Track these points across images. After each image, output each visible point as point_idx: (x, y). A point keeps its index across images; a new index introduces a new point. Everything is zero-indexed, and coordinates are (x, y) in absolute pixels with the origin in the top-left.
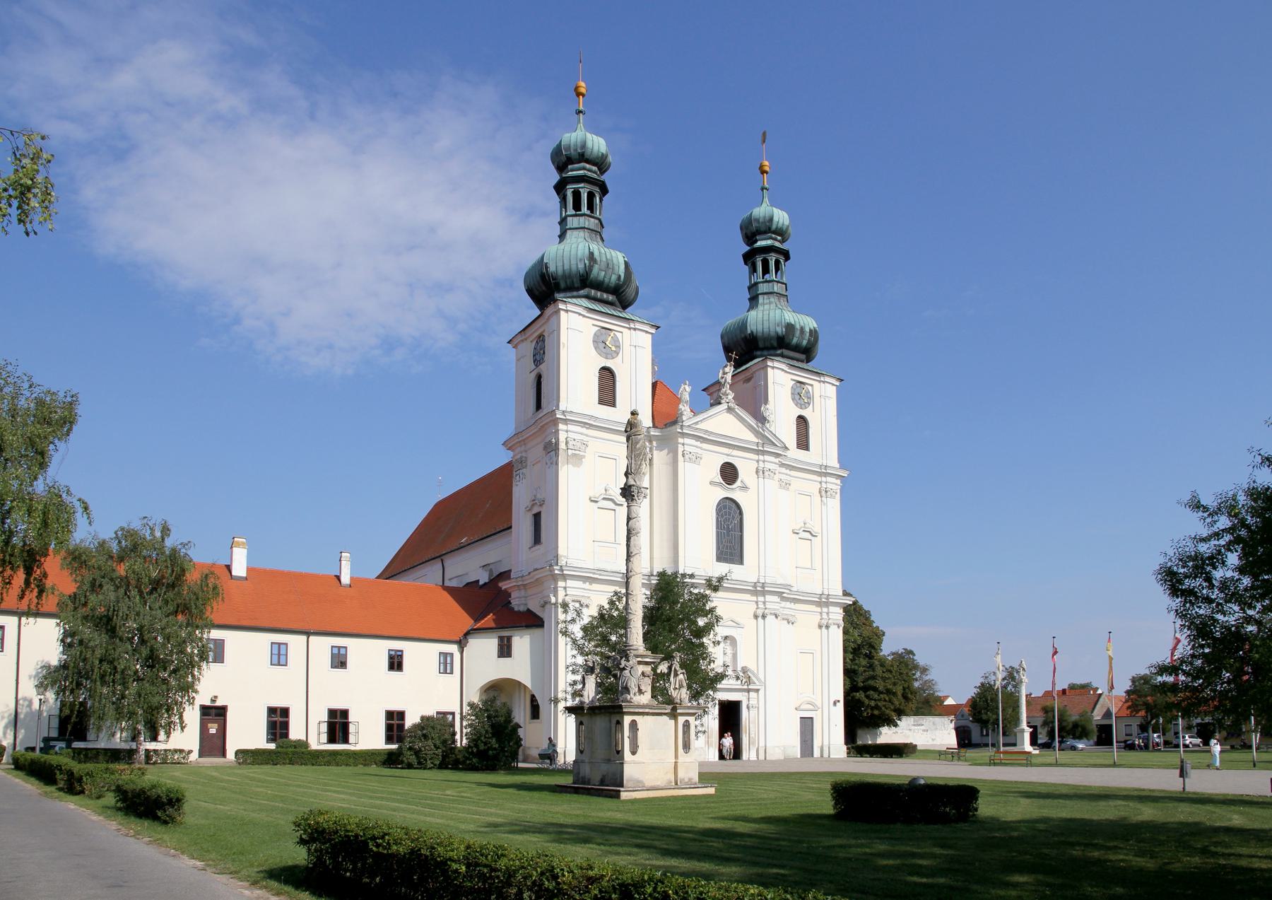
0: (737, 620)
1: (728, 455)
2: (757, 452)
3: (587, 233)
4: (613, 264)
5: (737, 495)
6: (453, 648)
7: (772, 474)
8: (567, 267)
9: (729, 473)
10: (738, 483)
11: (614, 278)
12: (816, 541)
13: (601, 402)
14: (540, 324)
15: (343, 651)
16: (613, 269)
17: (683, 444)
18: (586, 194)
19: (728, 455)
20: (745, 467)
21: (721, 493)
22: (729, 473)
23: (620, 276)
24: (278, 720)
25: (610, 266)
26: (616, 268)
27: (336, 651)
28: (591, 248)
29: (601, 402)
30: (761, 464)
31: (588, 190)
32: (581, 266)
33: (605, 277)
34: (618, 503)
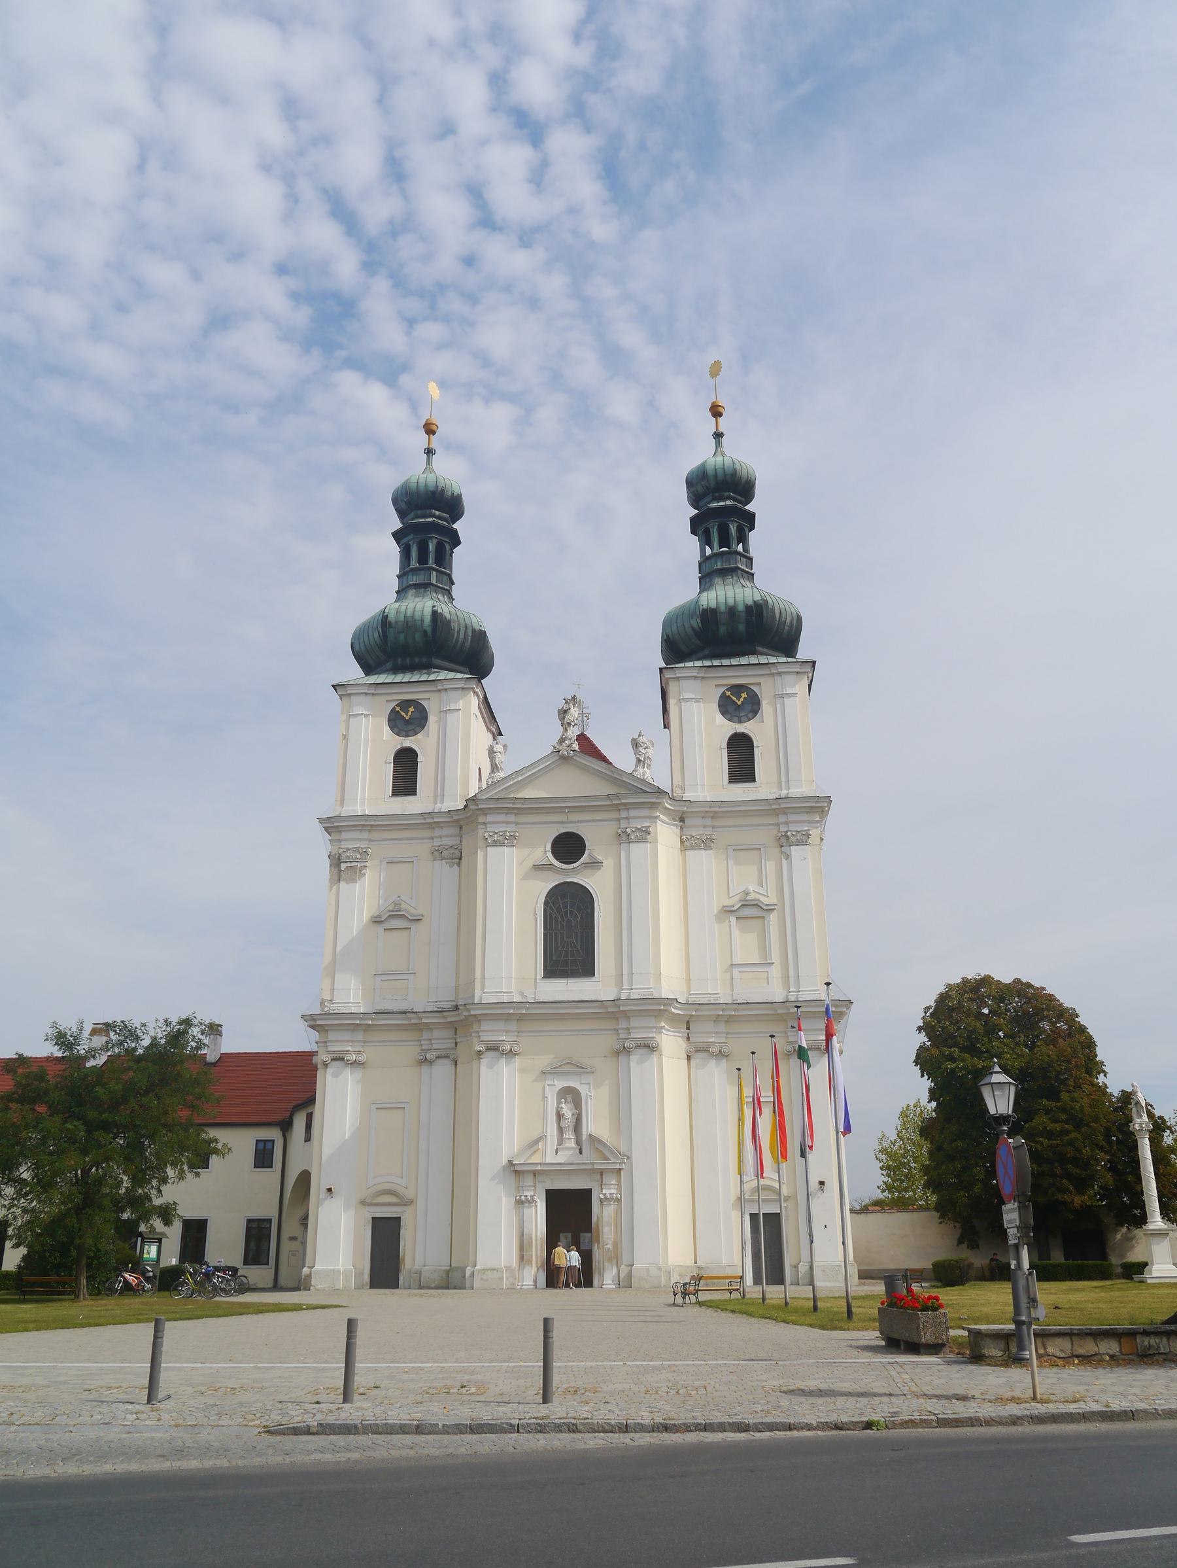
1: (562, 823)
2: (618, 808)
3: (412, 591)
6: (273, 1134)
7: (644, 834)
11: (417, 636)
12: (773, 918)
13: (396, 792)
15: (269, 1145)
17: (485, 823)
19: (562, 823)
23: (425, 632)
27: (261, 1146)
28: (387, 611)
29: (396, 792)
30: (624, 824)
31: (418, 540)
32: (376, 635)
33: (406, 638)
34: (411, 918)
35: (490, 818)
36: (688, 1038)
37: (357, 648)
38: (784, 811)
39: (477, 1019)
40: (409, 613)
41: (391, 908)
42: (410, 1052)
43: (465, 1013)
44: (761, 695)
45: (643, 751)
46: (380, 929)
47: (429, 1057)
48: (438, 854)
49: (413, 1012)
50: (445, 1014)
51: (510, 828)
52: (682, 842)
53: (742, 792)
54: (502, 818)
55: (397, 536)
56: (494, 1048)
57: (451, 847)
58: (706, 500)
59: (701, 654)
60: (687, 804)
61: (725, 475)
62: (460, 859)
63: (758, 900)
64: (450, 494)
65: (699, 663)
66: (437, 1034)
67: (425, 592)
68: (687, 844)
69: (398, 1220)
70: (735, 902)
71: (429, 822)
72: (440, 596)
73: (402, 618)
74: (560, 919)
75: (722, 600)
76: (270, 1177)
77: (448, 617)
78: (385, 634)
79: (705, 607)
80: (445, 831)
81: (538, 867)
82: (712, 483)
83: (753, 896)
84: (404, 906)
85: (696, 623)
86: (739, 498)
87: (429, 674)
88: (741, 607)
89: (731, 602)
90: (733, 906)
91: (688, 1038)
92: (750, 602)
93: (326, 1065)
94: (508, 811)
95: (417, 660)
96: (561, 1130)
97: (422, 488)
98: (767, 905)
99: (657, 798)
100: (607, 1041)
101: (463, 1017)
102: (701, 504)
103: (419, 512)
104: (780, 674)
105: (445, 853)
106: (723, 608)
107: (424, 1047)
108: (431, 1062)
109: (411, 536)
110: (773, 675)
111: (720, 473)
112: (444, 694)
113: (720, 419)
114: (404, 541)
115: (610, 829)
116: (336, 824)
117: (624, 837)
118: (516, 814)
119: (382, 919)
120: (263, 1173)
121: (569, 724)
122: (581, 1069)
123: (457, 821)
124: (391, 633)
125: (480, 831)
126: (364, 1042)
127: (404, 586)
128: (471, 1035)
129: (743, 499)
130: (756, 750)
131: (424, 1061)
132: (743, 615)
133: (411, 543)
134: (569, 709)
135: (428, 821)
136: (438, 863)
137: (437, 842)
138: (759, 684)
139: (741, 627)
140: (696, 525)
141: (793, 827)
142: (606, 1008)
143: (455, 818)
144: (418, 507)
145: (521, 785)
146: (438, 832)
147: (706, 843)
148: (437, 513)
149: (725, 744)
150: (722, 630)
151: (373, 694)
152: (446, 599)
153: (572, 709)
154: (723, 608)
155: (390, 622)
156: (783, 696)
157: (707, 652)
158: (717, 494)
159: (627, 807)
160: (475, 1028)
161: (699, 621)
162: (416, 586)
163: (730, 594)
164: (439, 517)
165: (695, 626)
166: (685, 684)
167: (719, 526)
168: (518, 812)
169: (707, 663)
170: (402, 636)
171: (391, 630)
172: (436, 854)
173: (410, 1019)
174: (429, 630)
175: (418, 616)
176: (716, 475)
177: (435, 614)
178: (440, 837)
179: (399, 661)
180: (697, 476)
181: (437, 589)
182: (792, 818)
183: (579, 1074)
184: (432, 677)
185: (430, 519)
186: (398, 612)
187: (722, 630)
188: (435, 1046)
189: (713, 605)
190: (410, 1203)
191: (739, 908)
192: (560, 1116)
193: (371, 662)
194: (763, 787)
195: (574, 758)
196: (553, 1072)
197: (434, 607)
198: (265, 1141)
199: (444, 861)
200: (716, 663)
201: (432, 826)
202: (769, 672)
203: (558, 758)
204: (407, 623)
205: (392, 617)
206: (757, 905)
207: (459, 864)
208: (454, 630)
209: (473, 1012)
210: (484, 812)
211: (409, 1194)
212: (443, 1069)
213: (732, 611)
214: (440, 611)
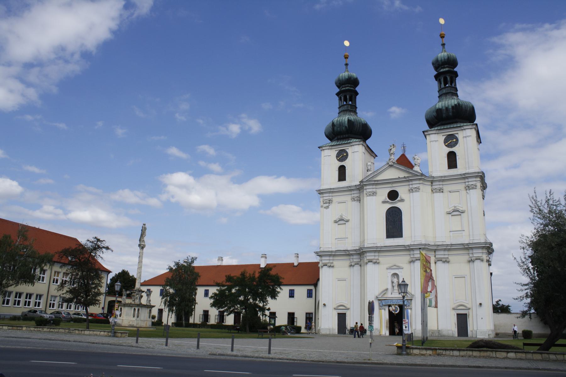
0: (397, 264)
2: (408, 181)
4: (342, 123)
5: (399, 205)
6: (312, 287)
7: (418, 190)
8: (328, 131)
9: (393, 195)
10: (399, 199)
11: (344, 128)
14: (368, 150)
16: (342, 125)
17: (366, 189)
18: (343, 97)
20: (402, 191)
21: (388, 206)
22: (393, 195)
23: (346, 127)
24: (291, 316)
25: (341, 125)
26: (344, 124)
28: (334, 121)
32: (331, 129)
33: (340, 129)
34: (346, 220)
35: (368, 187)
36: (435, 256)
37: (326, 134)
38: (467, 178)
39: (366, 252)
40: (341, 121)
41: (340, 217)
42: (347, 263)
43: (362, 250)
44: (459, 137)
45: (417, 161)
46: (336, 224)
47: (353, 264)
48: (353, 199)
49: (347, 250)
50: (357, 251)
51: (374, 190)
52: (432, 191)
53: (453, 172)
54: (371, 187)
55: (338, 94)
56: (370, 261)
57: (357, 197)
58: (439, 69)
59: (438, 124)
60: (433, 178)
61: (444, 59)
62: (360, 201)
63: (459, 209)
64: (353, 78)
65: (436, 128)
66: (355, 257)
67: (347, 113)
68: (434, 191)
69: (345, 314)
70: (450, 210)
71: (349, 189)
72: (352, 113)
73: (338, 122)
74: (391, 219)
75: (443, 105)
76: (312, 300)
77: (353, 120)
78: (333, 129)
79: (438, 108)
80: (355, 192)
81: (384, 202)
82: (440, 63)
83: (458, 207)
84: (343, 217)
85: (435, 114)
86: (451, 66)
87: (348, 140)
88: (450, 107)
89: (447, 105)
90: (450, 212)
91: (435, 256)
92: (453, 105)
93: (322, 267)
94: (373, 184)
95: (344, 136)
96: (393, 287)
97: (344, 78)
98: (462, 211)
99: (421, 177)
100: (408, 258)
101: (361, 252)
102: (438, 70)
103: (344, 86)
104: (465, 129)
105: (355, 199)
106: (444, 108)
107: (351, 261)
108: (353, 266)
109: (341, 95)
110: (462, 130)
111: (443, 59)
112: (353, 147)
113: (444, 39)
114: (340, 96)
115: (407, 188)
116: (321, 192)
117: (411, 191)
118: (376, 185)
119: (337, 221)
120: (310, 299)
121: (392, 154)
122: (399, 268)
123: (358, 188)
124: (335, 128)
125: (365, 192)
126: (333, 260)
127: (340, 111)
128: (364, 257)
129: (452, 67)
130: (457, 157)
131: (351, 266)
132: (451, 110)
133: (341, 97)
134: (392, 149)
135: (349, 189)
136: (353, 202)
137: (353, 196)
138: (458, 133)
139: (451, 114)
140: (437, 77)
141: (470, 183)
142: (406, 247)
143: (358, 187)
144: (343, 84)
145: (376, 175)
146: (353, 192)
147: (441, 191)
148: (349, 85)
149: (446, 156)
150: (444, 115)
151: (331, 149)
152: (354, 114)
153: (393, 149)
154: (444, 108)
155: (335, 125)
156: (466, 137)
157: (440, 123)
158: (442, 66)
159: (411, 180)
160: (365, 255)
161: (436, 113)
162: (344, 111)
163: (447, 102)
164: (350, 87)
165: (435, 115)
166: (431, 136)
167: (444, 78)
168: (376, 184)
169: (439, 128)
170: (339, 129)
171: (335, 127)
172: (353, 199)
173: (346, 252)
174: (347, 125)
175: (343, 121)
176: (441, 60)
177: (349, 121)
178: (354, 194)
179: (339, 137)
180: (435, 61)
181: (350, 111)
182: (470, 180)
183: (398, 269)
184: (349, 142)
185: (347, 88)
186: (337, 121)
187: (444, 115)
188: (354, 261)
189: (440, 107)
190: (348, 309)
191: (452, 212)
192: (393, 282)
193: (331, 138)
194: (461, 169)
195: (394, 165)
196: (390, 268)
197: (348, 118)
198: (310, 290)
199: (355, 202)
200: (442, 128)
201: (351, 190)
202: (460, 129)
203: (388, 166)
204: (340, 124)
205: (335, 122)
206: (458, 211)
207: (360, 202)
208: (355, 124)
209: (364, 250)
210: (366, 185)
211: (348, 306)
212: (357, 268)
213: (447, 109)
214: (350, 119)
